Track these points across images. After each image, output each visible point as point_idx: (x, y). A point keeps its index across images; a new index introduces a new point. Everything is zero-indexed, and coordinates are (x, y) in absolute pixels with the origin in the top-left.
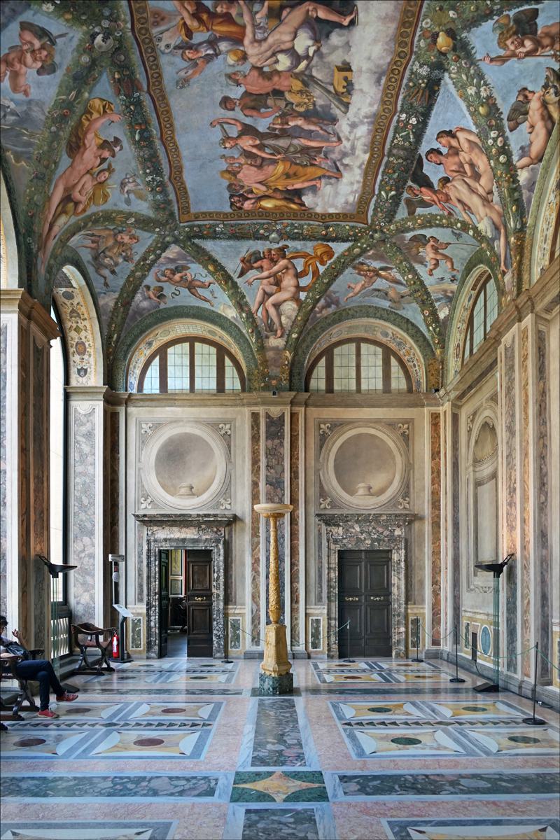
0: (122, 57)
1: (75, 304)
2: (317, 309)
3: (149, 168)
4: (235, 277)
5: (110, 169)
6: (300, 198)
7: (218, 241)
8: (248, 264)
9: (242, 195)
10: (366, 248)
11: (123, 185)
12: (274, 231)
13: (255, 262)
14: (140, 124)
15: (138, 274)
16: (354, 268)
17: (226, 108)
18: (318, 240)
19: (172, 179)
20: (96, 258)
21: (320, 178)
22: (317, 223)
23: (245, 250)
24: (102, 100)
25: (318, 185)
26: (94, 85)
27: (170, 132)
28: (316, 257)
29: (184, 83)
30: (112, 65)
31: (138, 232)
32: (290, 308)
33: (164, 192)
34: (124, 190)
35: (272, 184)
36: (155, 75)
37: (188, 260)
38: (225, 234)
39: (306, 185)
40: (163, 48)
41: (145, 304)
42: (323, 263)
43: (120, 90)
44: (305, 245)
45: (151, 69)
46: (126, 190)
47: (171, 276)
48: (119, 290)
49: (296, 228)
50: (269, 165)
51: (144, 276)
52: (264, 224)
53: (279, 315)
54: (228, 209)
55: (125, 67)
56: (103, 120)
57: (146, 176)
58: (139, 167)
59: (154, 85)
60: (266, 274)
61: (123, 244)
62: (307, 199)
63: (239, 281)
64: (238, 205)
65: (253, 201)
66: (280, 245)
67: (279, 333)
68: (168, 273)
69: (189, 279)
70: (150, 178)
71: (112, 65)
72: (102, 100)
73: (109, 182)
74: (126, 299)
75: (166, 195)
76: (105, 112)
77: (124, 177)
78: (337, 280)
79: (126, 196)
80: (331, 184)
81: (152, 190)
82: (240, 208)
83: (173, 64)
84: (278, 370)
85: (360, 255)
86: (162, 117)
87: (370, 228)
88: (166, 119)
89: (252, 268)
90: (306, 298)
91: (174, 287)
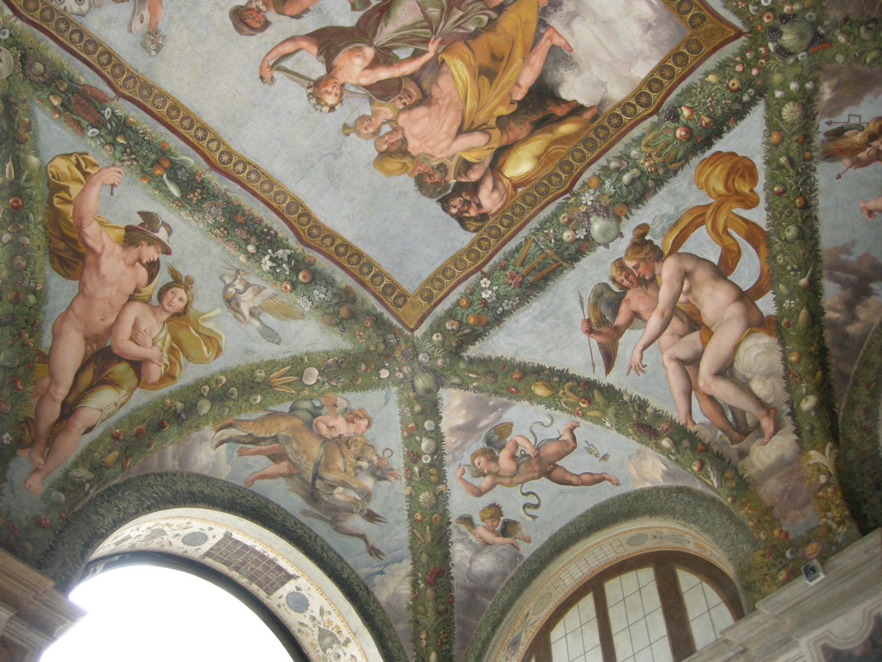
0: (39, 67)
1: (316, 614)
2: (830, 315)
3: (247, 242)
4: (599, 375)
5: (177, 280)
6: (559, 101)
7: (509, 323)
8: (604, 330)
9: (460, 188)
10: (801, 88)
11: (231, 302)
12: (587, 215)
13: (615, 314)
14: (157, 162)
15: (424, 497)
16: (830, 156)
17: (254, 30)
18: (686, 159)
19: (306, 238)
20: (312, 497)
21: (543, 23)
22: (646, 124)
23: (576, 303)
24: (67, 156)
25: (557, 41)
26: (35, 137)
27: (214, 145)
28: (722, 201)
29: (153, 39)
30: (36, 89)
31: (355, 399)
32: (759, 355)
33: (316, 277)
34: (242, 314)
35: (481, 117)
36: (104, 59)
37: (494, 409)
38: (507, 297)
39: (537, 60)
40: (76, 8)
41: (485, 563)
42: (749, 202)
43: (78, 123)
44: (674, 194)
45: (89, 53)
46: (247, 313)
47: (492, 466)
48: (406, 551)
49: (620, 171)
50: (435, 81)
51: (441, 499)
52: (555, 215)
53: (744, 386)
54: (465, 238)
55: (53, 80)
56: (95, 191)
57: (259, 261)
58: (230, 248)
59: (116, 77)
60: (654, 322)
61: (342, 442)
62: (574, 88)
63: (615, 379)
64: (473, 213)
65: (489, 182)
66: (629, 236)
67: (767, 424)
68: (481, 461)
69: (530, 451)
70: (267, 263)
71: (36, 89)
72: (67, 156)
73: (196, 306)
74: (435, 571)
75: (329, 283)
76: (86, 174)
77: (222, 285)
78: (821, 215)
79: (256, 323)
80: (573, 15)
81: (294, 286)
82: (483, 217)
83: (109, 21)
84: (810, 510)
85: (808, 116)
86: (176, 123)
87: (756, 37)
88: (186, 123)
89: (618, 332)
90: (779, 303)
91: (516, 491)
